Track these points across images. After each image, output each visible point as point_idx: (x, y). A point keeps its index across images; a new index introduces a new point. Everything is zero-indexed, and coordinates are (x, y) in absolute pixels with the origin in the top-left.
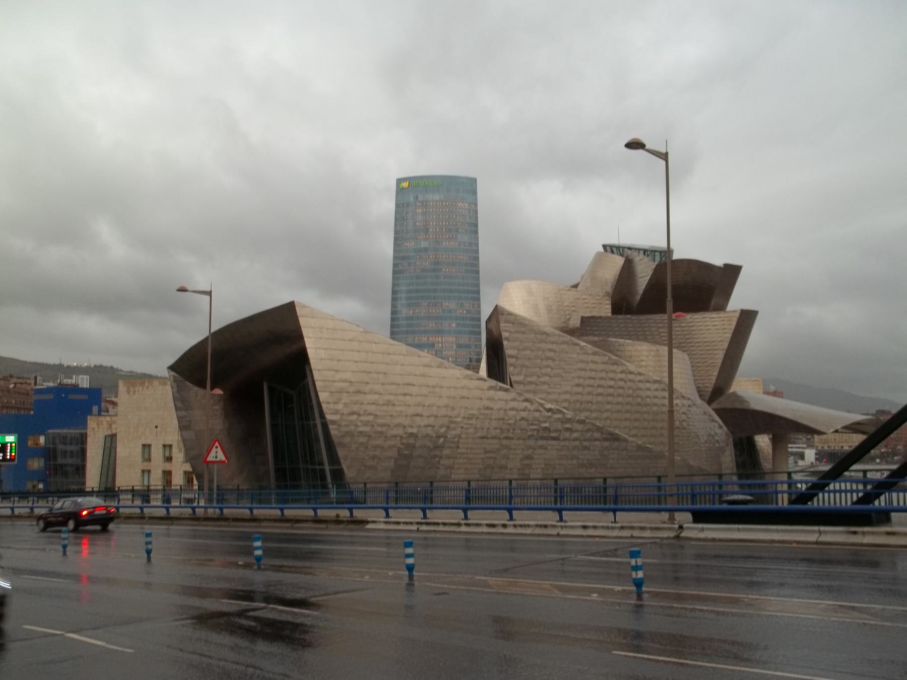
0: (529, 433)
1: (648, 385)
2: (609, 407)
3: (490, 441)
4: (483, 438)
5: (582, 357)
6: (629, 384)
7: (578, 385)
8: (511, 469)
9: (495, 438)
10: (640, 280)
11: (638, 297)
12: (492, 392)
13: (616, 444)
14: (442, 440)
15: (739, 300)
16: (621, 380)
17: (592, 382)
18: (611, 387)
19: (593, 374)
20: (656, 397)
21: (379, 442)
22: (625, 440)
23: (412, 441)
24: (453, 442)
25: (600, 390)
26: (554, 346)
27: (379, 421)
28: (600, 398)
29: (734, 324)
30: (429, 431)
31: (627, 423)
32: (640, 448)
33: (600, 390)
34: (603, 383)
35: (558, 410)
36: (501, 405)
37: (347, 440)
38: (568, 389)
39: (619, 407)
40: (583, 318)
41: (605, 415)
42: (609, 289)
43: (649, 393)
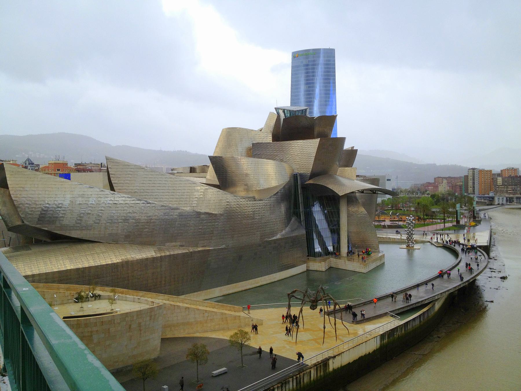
2: (158, 191)
5: (146, 173)
12: (86, 190)
13: (149, 205)
14: (61, 205)
19: (151, 179)
21: (34, 206)
23: (47, 205)
25: (153, 185)
26: (132, 170)
27: (34, 199)
28: (153, 188)
30: (56, 202)
31: (167, 197)
32: (162, 206)
33: (153, 185)
34: (155, 182)
37: (20, 206)
38: (138, 185)
39: (162, 191)
40: (253, 144)
41: (156, 194)
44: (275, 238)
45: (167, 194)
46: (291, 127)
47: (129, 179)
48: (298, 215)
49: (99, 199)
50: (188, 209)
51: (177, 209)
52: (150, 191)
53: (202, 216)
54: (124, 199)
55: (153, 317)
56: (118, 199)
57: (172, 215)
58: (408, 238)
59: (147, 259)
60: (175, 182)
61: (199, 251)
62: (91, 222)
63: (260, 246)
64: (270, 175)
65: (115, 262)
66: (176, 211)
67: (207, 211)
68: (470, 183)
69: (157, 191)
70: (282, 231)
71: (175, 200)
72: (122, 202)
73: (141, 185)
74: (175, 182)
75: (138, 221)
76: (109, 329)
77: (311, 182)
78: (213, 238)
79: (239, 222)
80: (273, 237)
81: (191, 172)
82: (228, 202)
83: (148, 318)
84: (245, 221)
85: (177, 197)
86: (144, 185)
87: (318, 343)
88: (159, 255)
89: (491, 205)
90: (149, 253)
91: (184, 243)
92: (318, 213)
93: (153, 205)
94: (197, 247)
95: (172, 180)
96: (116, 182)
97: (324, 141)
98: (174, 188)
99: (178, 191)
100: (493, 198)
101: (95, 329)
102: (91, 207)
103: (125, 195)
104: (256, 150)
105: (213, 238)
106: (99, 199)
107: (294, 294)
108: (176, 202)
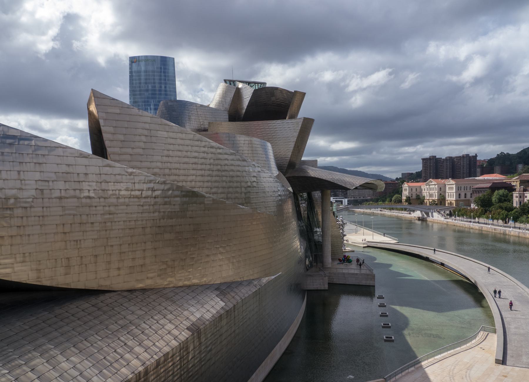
0: (110, 192)
1: (226, 156)
3: (69, 200)
4: (60, 198)
6: (210, 156)
8: (92, 223)
9: (75, 197)
10: (245, 100)
11: (244, 111)
14: (12, 201)
15: (303, 113)
16: (204, 152)
17: (179, 153)
18: (195, 158)
19: (181, 148)
20: (232, 165)
22: (203, 196)
24: (26, 202)
25: (186, 160)
26: (147, 126)
28: (185, 166)
29: (300, 126)
33: (186, 160)
35: (139, 173)
38: (159, 158)
42: (227, 106)
43: (226, 162)
45: (209, 178)
47: (142, 145)
49: (104, 186)
52: (182, 172)
60: (220, 156)
71: (220, 190)
73: (165, 159)
74: (220, 156)
82: (280, 195)
86: (170, 159)
95: (213, 150)
96: (117, 150)
98: (219, 167)
99: (223, 173)
106: (104, 186)
108: (222, 195)
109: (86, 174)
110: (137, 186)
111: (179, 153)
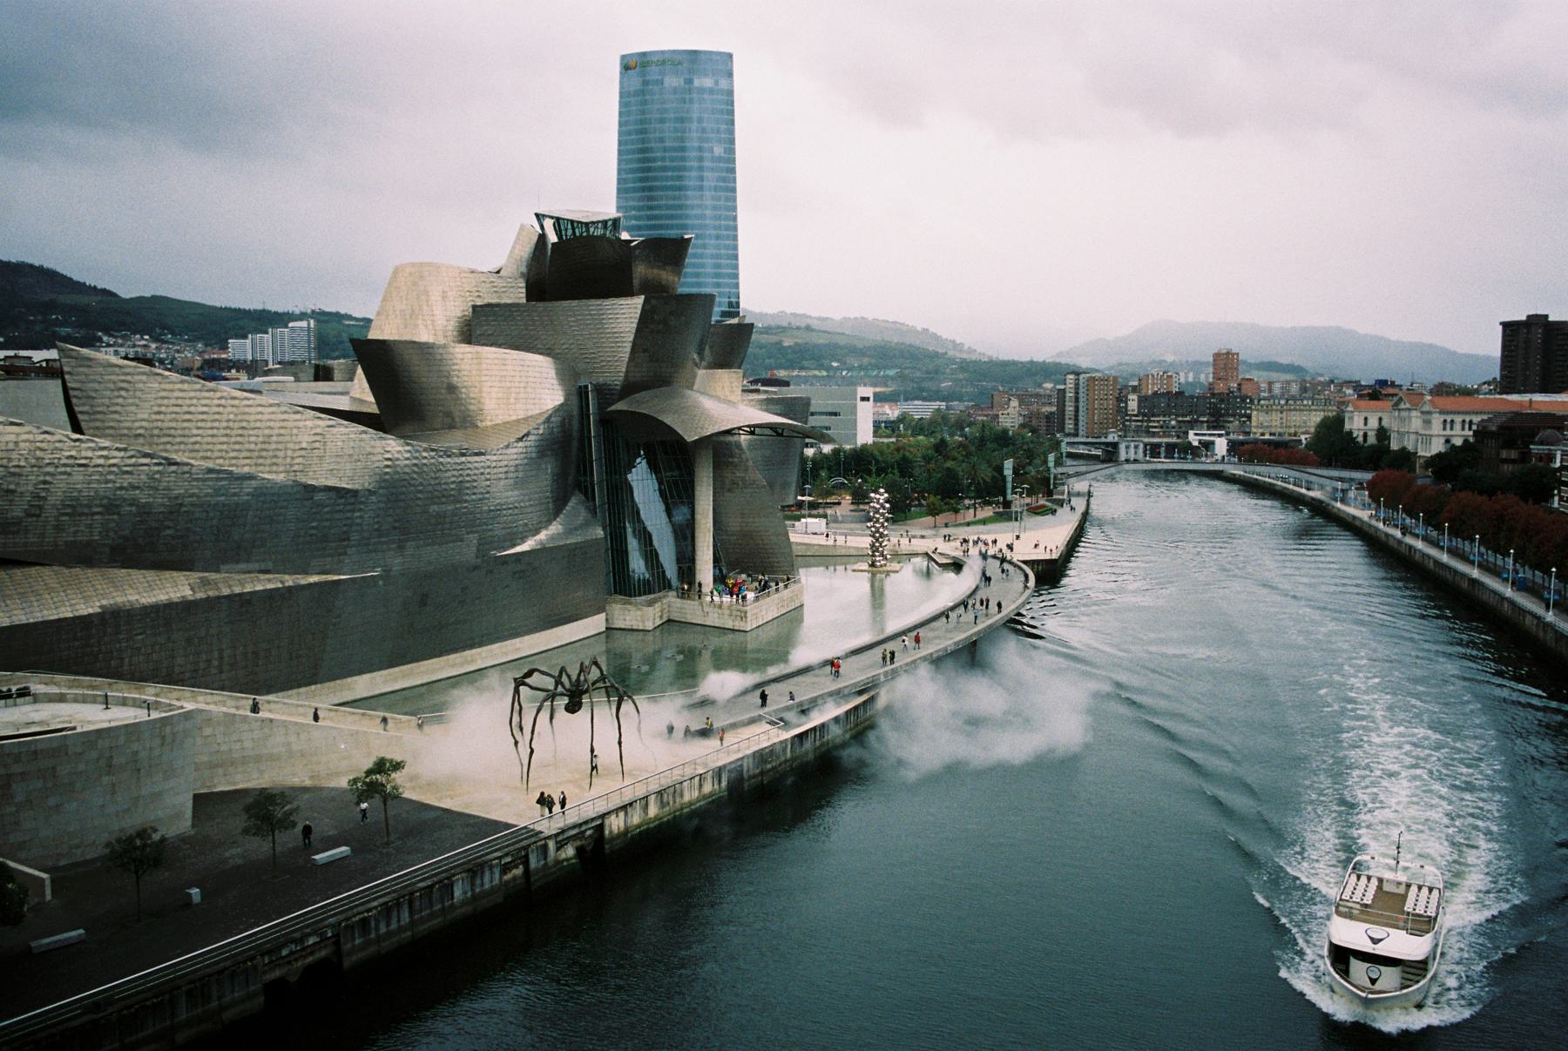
7: (159, 413)
13: (173, 468)
17: (177, 409)
25: (187, 417)
31: (224, 447)
32: (210, 471)
33: (187, 417)
34: (192, 409)
36: (13, 438)
38: (146, 416)
40: (474, 307)
42: (524, 269)
44: (518, 549)
46: (571, 267)
47: (120, 401)
48: (588, 495)
50: (281, 477)
51: (251, 477)
53: (319, 497)
54: (105, 453)
55: (168, 740)
56: (90, 454)
57: (235, 494)
58: (873, 546)
59: (170, 605)
61: (310, 585)
62: (17, 512)
63: (476, 568)
64: (516, 392)
65: (85, 613)
66: (246, 483)
67: (330, 483)
68: (1070, 409)
69: (195, 432)
70: (537, 532)
72: (101, 461)
75: (144, 511)
76: (54, 768)
77: (620, 406)
78: (349, 551)
79: (418, 510)
80: (514, 546)
81: (317, 379)
83: (157, 741)
84: (435, 507)
85: (252, 446)
87: (580, 787)
88: (200, 595)
89: (1110, 461)
90: (175, 588)
91: (270, 565)
92: (642, 482)
93: (186, 469)
94: (306, 573)
97: (654, 302)
100: (1115, 445)
101: (16, 769)
102: (14, 474)
103: (107, 443)
104: (483, 324)
105: (349, 551)
107: (527, 680)
109: (16, 443)
110: (84, 454)
111: (177, 409)
